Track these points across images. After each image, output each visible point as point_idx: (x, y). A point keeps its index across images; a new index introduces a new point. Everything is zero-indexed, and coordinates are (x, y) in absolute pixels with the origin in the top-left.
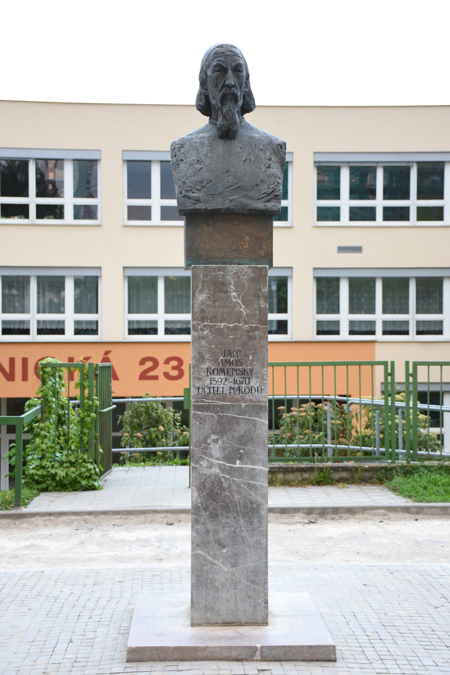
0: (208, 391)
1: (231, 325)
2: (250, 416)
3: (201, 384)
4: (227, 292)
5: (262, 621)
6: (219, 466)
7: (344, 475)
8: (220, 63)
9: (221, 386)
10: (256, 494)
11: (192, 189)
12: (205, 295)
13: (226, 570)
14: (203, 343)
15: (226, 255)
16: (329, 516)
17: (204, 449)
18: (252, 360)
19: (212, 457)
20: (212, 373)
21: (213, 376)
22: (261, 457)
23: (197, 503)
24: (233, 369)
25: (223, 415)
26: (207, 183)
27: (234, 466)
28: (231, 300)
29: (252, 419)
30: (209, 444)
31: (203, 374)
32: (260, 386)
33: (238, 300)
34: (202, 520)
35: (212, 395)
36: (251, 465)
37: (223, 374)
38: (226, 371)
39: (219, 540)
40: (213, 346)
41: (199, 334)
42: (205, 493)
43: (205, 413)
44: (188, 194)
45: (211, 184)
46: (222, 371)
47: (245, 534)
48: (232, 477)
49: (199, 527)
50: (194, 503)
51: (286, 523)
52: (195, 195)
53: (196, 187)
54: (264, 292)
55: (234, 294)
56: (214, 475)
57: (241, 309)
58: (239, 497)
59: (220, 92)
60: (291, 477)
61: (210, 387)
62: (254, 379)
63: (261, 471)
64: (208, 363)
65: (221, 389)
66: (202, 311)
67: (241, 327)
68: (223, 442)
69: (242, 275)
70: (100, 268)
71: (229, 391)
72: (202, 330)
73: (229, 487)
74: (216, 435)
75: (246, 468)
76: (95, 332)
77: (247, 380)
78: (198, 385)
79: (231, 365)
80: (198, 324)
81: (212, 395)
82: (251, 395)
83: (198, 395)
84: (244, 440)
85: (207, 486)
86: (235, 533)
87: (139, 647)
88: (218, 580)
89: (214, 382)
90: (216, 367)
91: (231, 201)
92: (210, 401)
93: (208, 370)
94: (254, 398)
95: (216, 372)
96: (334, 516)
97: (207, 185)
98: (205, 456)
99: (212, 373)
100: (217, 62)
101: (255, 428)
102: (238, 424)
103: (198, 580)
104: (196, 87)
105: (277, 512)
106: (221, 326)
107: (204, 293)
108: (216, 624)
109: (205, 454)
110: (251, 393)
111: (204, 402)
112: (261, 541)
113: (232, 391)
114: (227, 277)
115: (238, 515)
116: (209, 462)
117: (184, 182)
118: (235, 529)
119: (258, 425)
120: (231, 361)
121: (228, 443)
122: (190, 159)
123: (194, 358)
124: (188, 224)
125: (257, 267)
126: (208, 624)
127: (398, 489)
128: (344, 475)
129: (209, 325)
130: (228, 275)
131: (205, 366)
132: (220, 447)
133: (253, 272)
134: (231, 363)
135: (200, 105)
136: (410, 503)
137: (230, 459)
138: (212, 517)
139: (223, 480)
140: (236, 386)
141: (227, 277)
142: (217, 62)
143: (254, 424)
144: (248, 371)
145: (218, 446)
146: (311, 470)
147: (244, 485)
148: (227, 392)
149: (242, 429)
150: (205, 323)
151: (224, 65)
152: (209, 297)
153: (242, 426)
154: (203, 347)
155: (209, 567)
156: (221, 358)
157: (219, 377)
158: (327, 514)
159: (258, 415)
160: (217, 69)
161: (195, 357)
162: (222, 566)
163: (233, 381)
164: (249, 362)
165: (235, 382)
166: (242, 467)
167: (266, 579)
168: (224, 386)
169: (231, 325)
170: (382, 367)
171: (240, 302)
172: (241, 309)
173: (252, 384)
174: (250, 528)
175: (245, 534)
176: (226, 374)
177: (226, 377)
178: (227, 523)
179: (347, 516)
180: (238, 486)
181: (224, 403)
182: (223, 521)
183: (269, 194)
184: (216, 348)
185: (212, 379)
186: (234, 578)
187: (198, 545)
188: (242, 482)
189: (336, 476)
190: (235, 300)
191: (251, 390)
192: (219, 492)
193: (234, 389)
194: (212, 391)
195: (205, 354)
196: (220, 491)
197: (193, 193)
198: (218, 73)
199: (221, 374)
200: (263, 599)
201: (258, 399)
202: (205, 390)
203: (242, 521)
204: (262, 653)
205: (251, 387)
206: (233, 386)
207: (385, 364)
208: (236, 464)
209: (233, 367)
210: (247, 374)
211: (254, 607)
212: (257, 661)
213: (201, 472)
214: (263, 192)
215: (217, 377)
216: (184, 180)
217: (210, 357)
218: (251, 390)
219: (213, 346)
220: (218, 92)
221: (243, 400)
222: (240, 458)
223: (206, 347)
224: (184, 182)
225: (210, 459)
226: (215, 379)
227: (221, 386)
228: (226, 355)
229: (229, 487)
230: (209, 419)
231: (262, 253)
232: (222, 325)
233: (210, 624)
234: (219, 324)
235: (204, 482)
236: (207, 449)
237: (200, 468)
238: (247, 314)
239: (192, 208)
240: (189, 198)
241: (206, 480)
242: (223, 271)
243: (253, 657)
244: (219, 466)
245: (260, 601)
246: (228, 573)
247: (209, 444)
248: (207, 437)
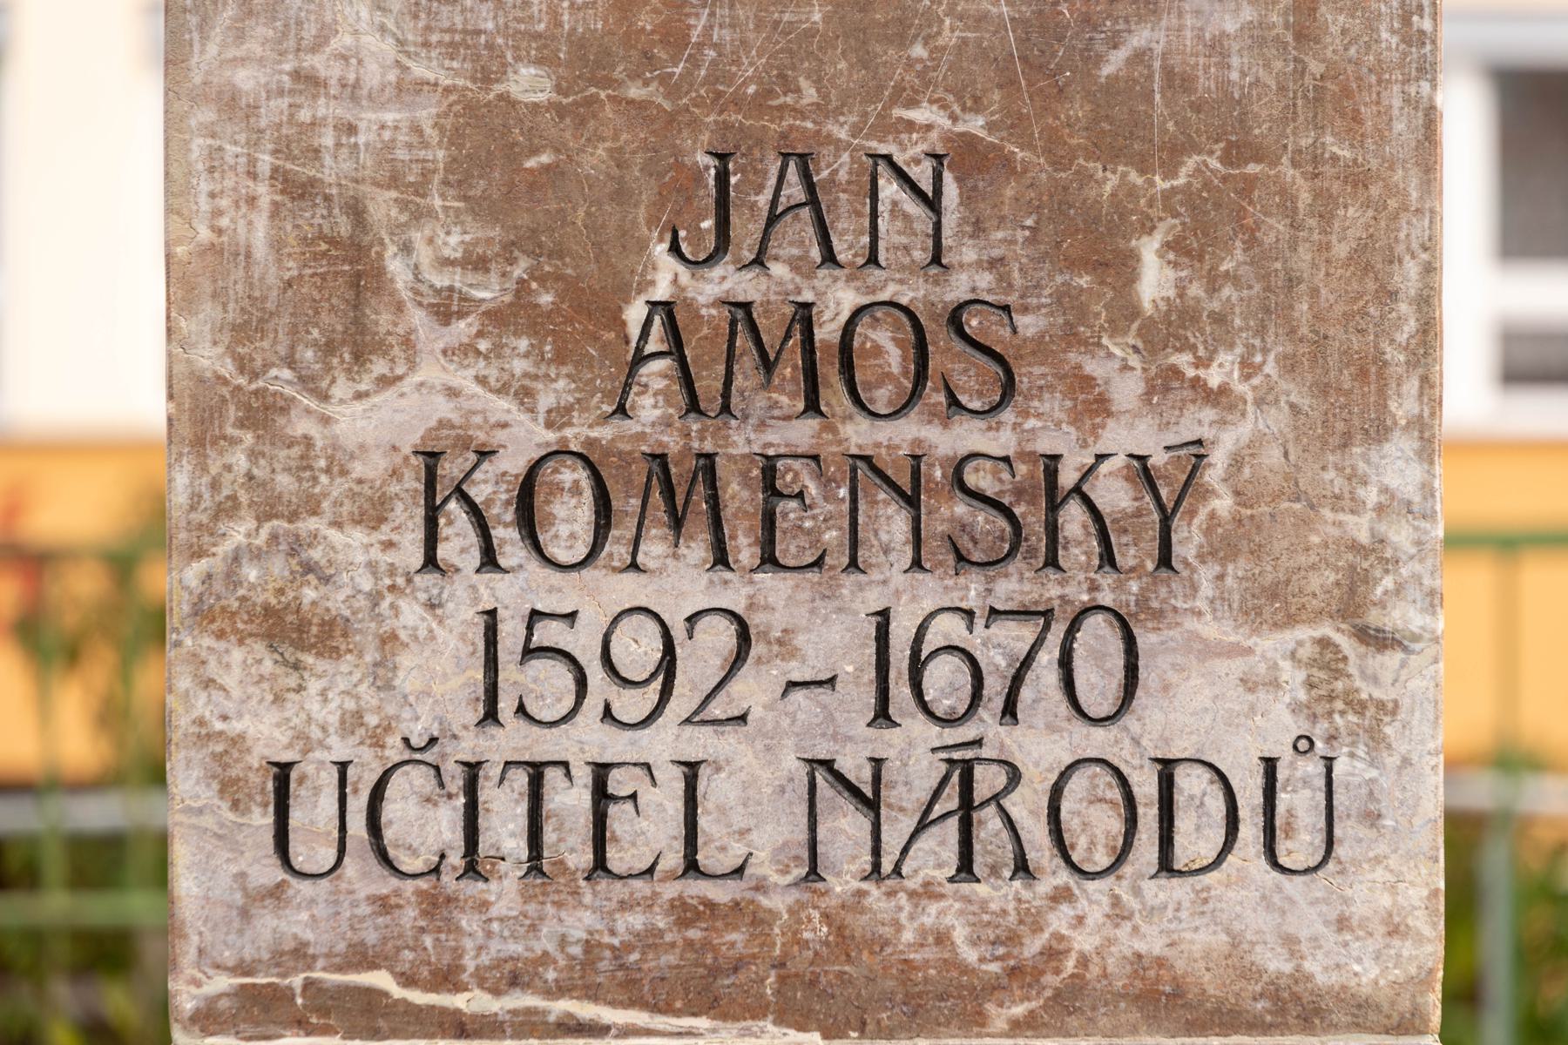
0: (446, 825)
20: (506, 535)
21: (521, 586)
32: (1303, 745)
35: (505, 891)
37: (697, 550)
38: (739, 495)
40: (528, 83)
46: (681, 493)
64: (431, 371)
65: (666, 798)
78: (266, 735)
79: (834, 396)
82: (1178, 890)
89: (548, 685)
90: (575, 434)
93: (437, 479)
95: (569, 521)
99: (506, 535)
110: (1166, 865)
113: (845, 828)
120: (827, 332)
131: (373, 422)
134: (821, 366)
144: (1114, 494)
154: (352, 91)
157: (630, 590)
161: (223, 254)
163: (856, 666)
165: (895, 674)
168: (699, 744)
176: (745, 550)
177: (735, 599)
184: (576, 113)
185: (511, 634)
193: (871, 804)
194: (505, 828)
195: (382, 206)
199: (654, 549)
201: (1276, 963)
205: (1167, 769)
209: (859, 434)
210: (1081, 552)
215: (606, 591)
217: (476, 262)
221: (1020, 975)
226: (547, 633)
227: (665, 743)
228: (746, 230)
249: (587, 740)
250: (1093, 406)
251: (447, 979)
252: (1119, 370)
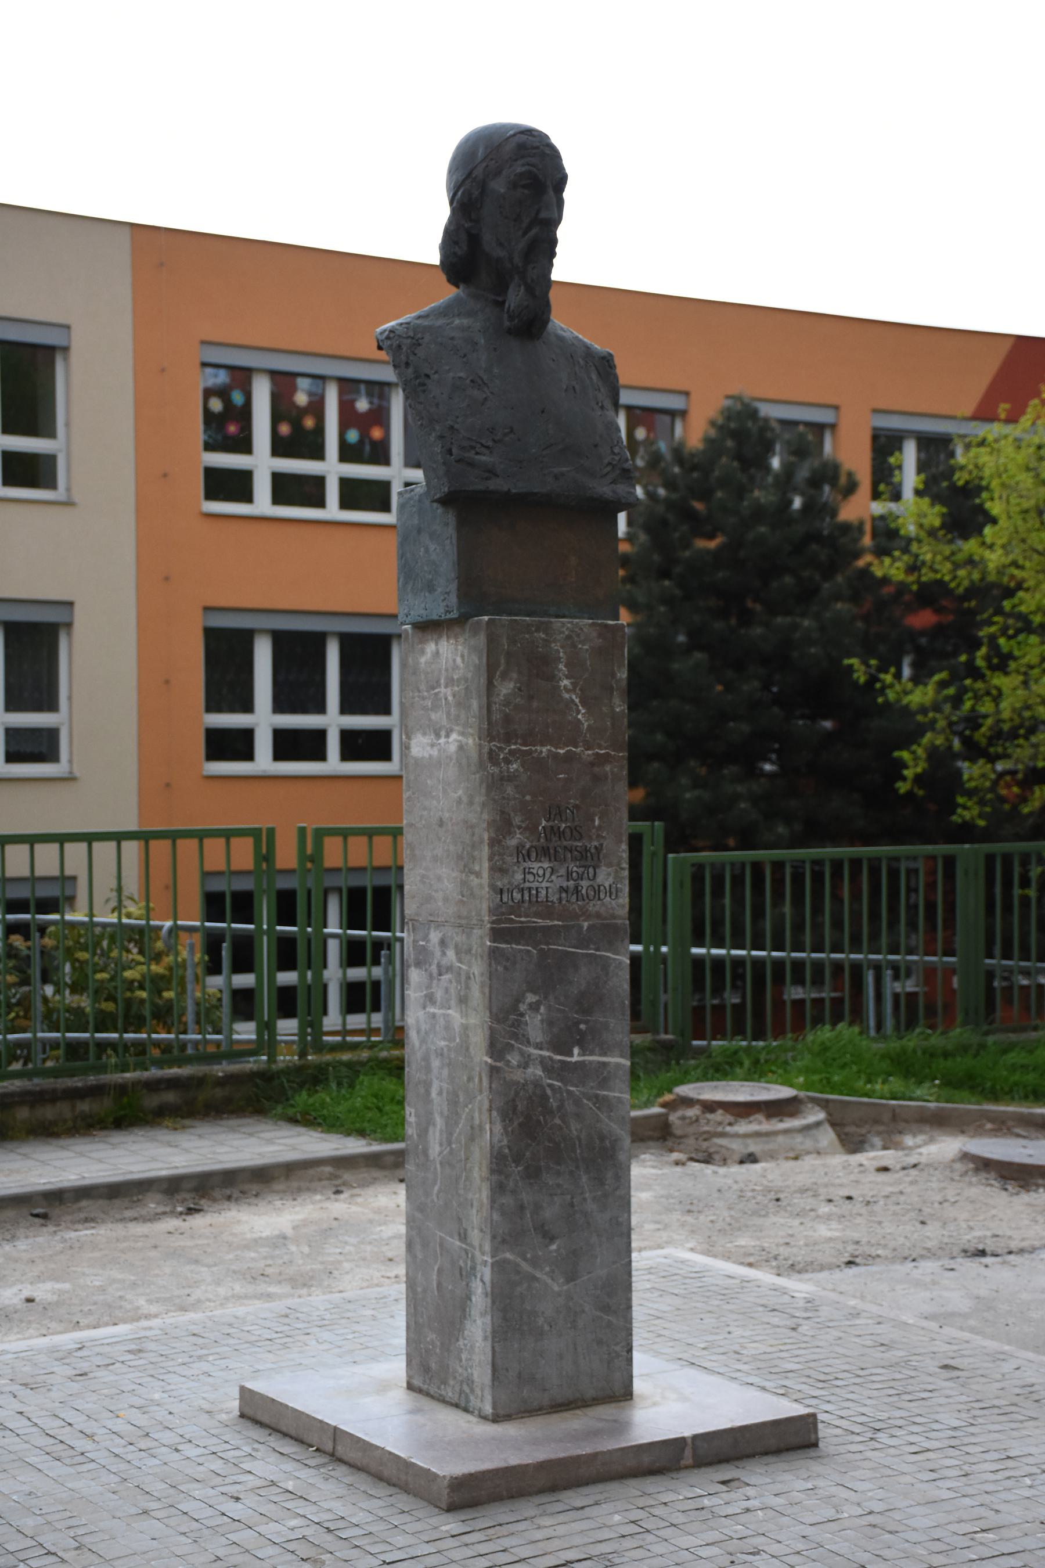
1: (561, 751)
2: (597, 950)
3: (506, 881)
5: (622, 1391)
6: (542, 1061)
7: (170, 1097)
8: (532, 168)
9: (544, 885)
10: (609, 1117)
11: (474, 444)
12: (512, 685)
13: (556, 1288)
14: (510, 790)
16: (217, 1193)
17: (513, 1026)
18: (600, 828)
19: (529, 1042)
22: (618, 1037)
23: (501, 1147)
24: (565, 847)
25: (549, 949)
26: (505, 435)
27: (569, 1059)
28: (560, 696)
29: (601, 956)
30: (522, 1015)
31: (508, 859)
33: (574, 697)
34: (511, 1184)
35: (526, 905)
36: (600, 1055)
38: (552, 851)
39: (543, 1225)
40: (528, 798)
41: (501, 772)
42: (516, 1123)
43: (514, 946)
44: (466, 455)
45: (512, 436)
46: (544, 852)
47: (591, 1206)
48: (565, 1085)
49: (504, 1200)
50: (496, 1148)
51: (135, 1219)
52: (483, 458)
53: (483, 441)
55: (566, 682)
57: (580, 717)
58: (578, 1127)
59: (525, 233)
60: (49, 1112)
61: (523, 889)
62: (604, 868)
63: (618, 1066)
64: (518, 836)
65: (544, 892)
66: (507, 719)
67: (579, 754)
68: (549, 1008)
69: (580, 642)
70: (70, 604)
71: (557, 896)
72: (508, 762)
73: (561, 1107)
74: (535, 993)
75: (591, 1062)
77: (591, 870)
80: (500, 749)
81: (526, 905)
83: (501, 906)
84: (589, 1002)
85: (519, 1107)
86: (572, 1205)
87: (471, 1475)
88: (543, 1313)
89: (530, 877)
90: (534, 844)
91: (556, 477)
92: (523, 919)
93: (519, 849)
94: (603, 908)
95: (534, 855)
96: (228, 1192)
97: (507, 439)
98: (516, 1041)
100: (527, 168)
101: (607, 974)
103: (505, 1319)
104: (440, 212)
105: (100, 1197)
106: (541, 752)
107: (511, 679)
108: (540, 1409)
109: (515, 1036)
111: (511, 921)
112: (620, 1219)
113: (564, 895)
114: (553, 645)
115: (577, 1167)
116: (522, 1053)
117: (452, 427)
118: (572, 1198)
119: (612, 968)
121: (559, 1010)
122: (451, 374)
123: (491, 824)
124: (462, 523)
125: (606, 626)
126: (525, 1412)
127: (315, 1118)
128: (170, 1097)
129: (520, 750)
130: (555, 641)
131: (513, 842)
132: (542, 1021)
133: (600, 635)
134: (561, 834)
135: (455, 253)
136: (355, 1146)
137: (562, 1046)
139: (549, 1092)
140: (571, 883)
141: (553, 645)
142: (527, 168)
143: (605, 965)
144: (593, 850)
145: (539, 1017)
146: (96, 1091)
147: (588, 1099)
148: (554, 898)
149: (581, 978)
150: (513, 747)
151: (541, 176)
152: (520, 689)
153: (584, 970)
154: (508, 799)
155: (525, 1285)
156: (544, 823)
157: (540, 865)
158: (212, 1188)
159: (611, 947)
160: (524, 182)
161: (494, 821)
162: (549, 1281)
164: (594, 831)
165: (569, 876)
166: (584, 1061)
167: (630, 1300)
168: (548, 884)
169: (561, 751)
170: (249, 842)
171: (577, 701)
172: (580, 717)
173: (600, 879)
174: (599, 1193)
175: (591, 1206)
178: (559, 1186)
179: (255, 1188)
180: (577, 1102)
181: (549, 923)
182: (551, 1183)
186: (571, 1304)
187: (503, 1241)
188: (583, 1093)
189: (152, 1101)
190: (567, 696)
191: (597, 891)
192: (541, 1118)
195: (512, 814)
196: (544, 1117)
197: (477, 453)
198: (526, 191)
200: (624, 1344)
202: (515, 894)
203: (584, 1179)
204: (694, 1449)
206: (565, 884)
207: (255, 833)
208: (572, 1055)
209: (565, 843)
211: (609, 1363)
212: (687, 1467)
213: (508, 1078)
215: (536, 865)
216: (450, 423)
217: (522, 821)
218: (597, 891)
219: (528, 798)
220: (520, 233)
222: (581, 1043)
223: (515, 799)
224: (452, 427)
225: (524, 1048)
227: (544, 885)
229: (561, 1107)
230: (522, 959)
232: (544, 749)
233: (529, 1412)
234: (538, 748)
235: (514, 1100)
236: (519, 1026)
237: (506, 1069)
238: (589, 726)
239: (481, 487)
240: (471, 464)
241: (517, 1094)
243: (679, 1461)
244: (541, 1062)
245: (618, 1348)
246: (560, 1295)
247: (522, 1015)
248: (519, 1000)
249: (535, 885)
251: (520, 916)
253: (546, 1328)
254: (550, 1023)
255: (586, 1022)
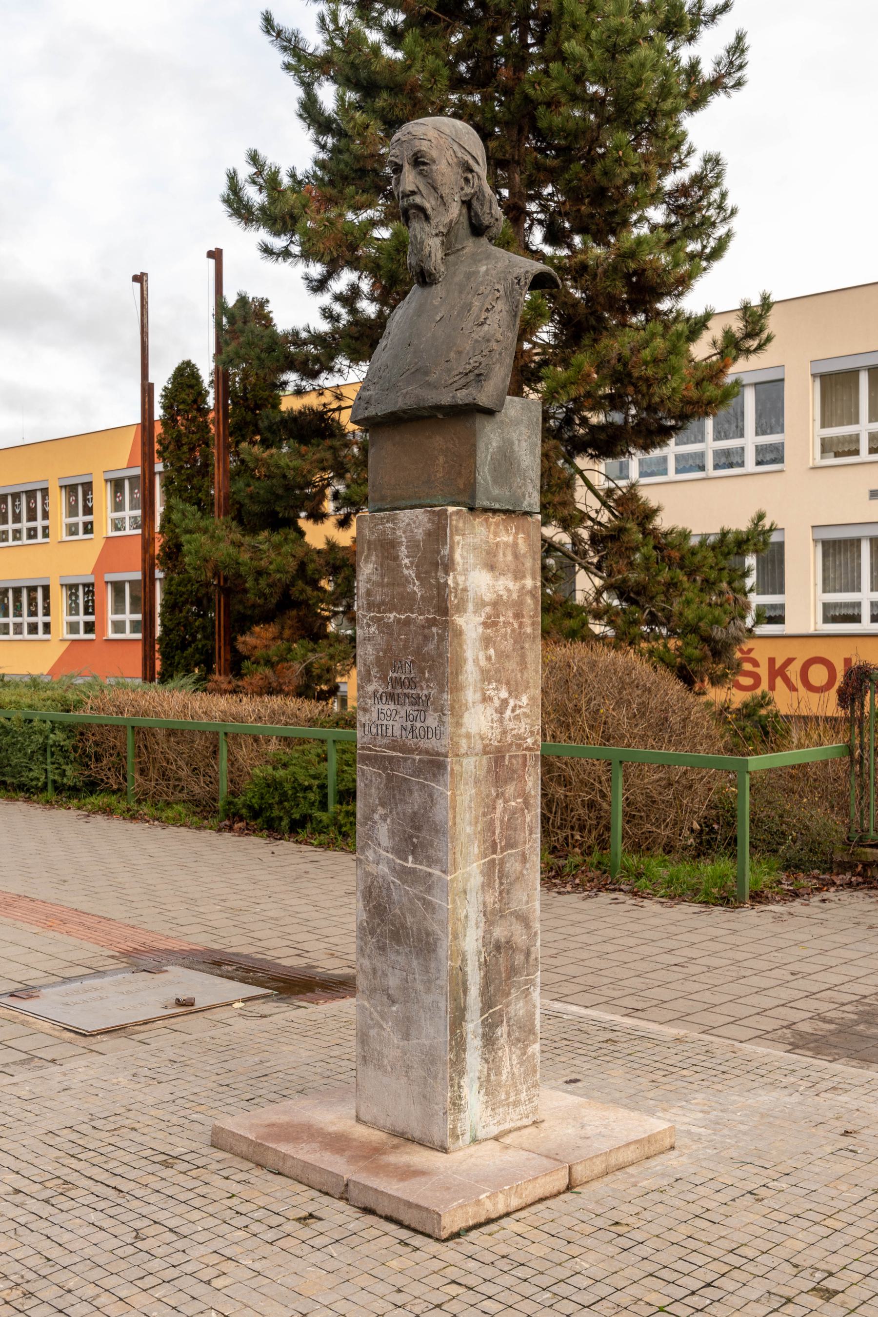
2: (426, 779)
4: (398, 557)
6: (389, 861)
9: (391, 723)
10: (433, 919)
15: (415, 492)
21: (381, 706)
29: (428, 786)
46: (391, 697)
47: (420, 987)
54: (444, 556)
55: (406, 561)
56: (383, 877)
72: (369, 626)
75: (421, 870)
76: (779, 620)
95: (384, 699)
102: (411, 792)
111: (370, 749)
116: (375, 852)
130: (399, 528)
131: (370, 688)
138: (379, 948)
139: (392, 886)
148: (397, 733)
165: (408, 715)
175: (420, 987)
181: (394, 754)
183: (467, 374)
214: (456, 372)
215: (386, 707)
231: (461, 483)
242: (393, 520)
247: (375, 822)
249: (385, 722)
250: (422, 689)
252: (424, 684)
253: (389, 1069)
254: (393, 833)
255: (417, 837)
